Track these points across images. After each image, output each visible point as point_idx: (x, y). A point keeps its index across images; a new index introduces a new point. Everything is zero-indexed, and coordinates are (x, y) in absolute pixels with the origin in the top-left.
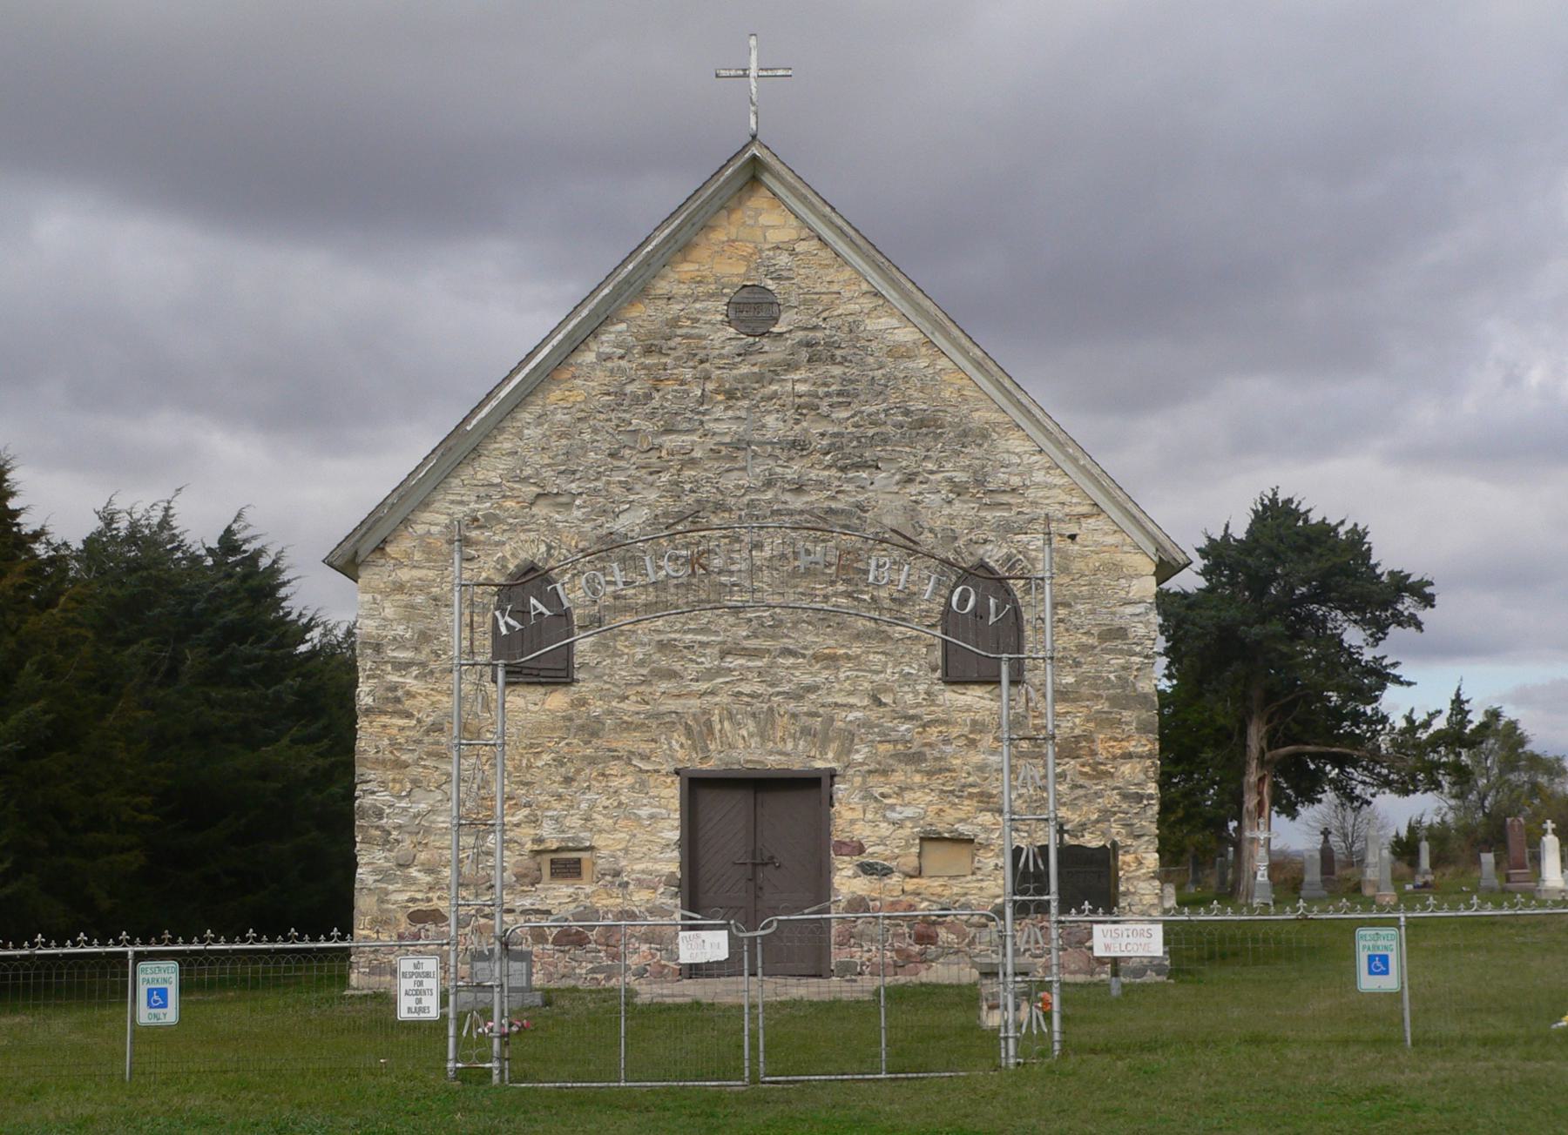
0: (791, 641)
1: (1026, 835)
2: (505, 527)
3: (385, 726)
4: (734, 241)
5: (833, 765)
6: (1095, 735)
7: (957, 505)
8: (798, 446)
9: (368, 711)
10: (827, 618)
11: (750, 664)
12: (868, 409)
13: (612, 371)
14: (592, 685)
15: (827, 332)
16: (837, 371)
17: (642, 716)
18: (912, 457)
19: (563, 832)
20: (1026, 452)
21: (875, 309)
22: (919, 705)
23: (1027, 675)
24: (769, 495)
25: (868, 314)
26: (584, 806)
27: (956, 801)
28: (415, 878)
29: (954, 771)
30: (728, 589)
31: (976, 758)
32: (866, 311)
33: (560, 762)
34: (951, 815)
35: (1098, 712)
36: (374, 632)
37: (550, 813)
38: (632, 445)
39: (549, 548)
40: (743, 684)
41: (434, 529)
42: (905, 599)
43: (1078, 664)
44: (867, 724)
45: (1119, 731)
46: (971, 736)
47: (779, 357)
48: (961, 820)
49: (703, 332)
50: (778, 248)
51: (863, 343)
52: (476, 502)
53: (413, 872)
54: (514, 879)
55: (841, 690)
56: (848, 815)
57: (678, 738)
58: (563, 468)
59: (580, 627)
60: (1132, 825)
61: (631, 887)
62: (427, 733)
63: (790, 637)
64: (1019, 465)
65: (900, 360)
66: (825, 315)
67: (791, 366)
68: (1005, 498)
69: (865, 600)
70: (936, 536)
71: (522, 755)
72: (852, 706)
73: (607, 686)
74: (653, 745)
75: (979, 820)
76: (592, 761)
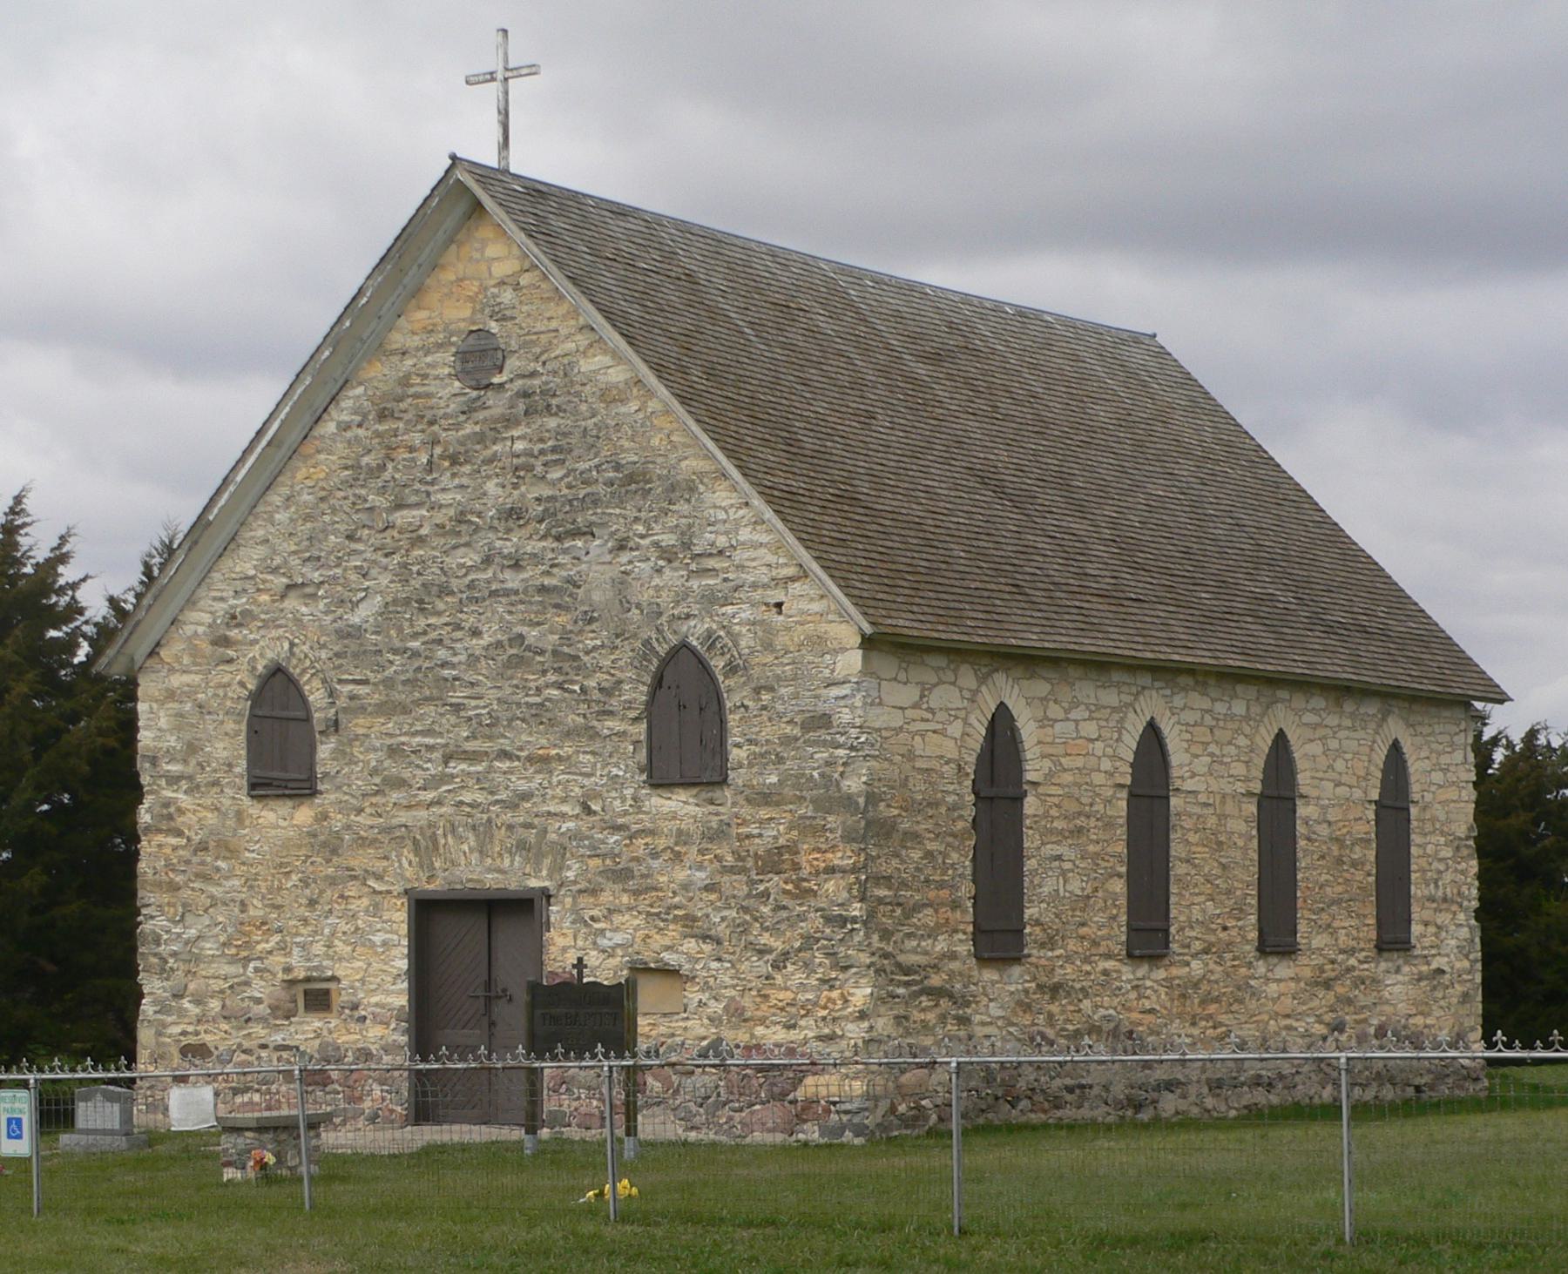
0: (507, 742)
1: (729, 965)
2: (260, 624)
3: (160, 846)
4: (462, 280)
5: (547, 884)
6: (800, 845)
7: (667, 572)
8: (513, 514)
9: (148, 829)
10: (540, 715)
11: (472, 769)
12: (582, 466)
13: (349, 442)
14: (332, 797)
15: (544, 378)
16: (552, 423)
17: (376, 831)
18: (622, 520)
19: (309, 960)
20: (732, 506)
21: (591, 345)
22: (626, 813)
23: (731, 774)
24: (490, 574)
25: (584, 353)
26: (327, 931)
27: (662, 924)
28: (186, 1010)
29: (661, 890)
30: (449, 685)
31: (681, 875)
32: (581, 349)
33: (305, 883)
34: (658, 941)
35: (802, 817)
36: (152, 744)
37: (298, 939)
38: (370, 524)
39: (292, 645)
40: (464, 792)
41: (201, 630)
42: (613, 689)
43: (780, 760)
44: (576, 836)
45: (822, 840)
46: (677, 848)
47: (497, 411)
48: (668, 948)
49: (432, 389)
50: (504, 283)
51: (578, 388)
52: (234, 598)
53: (185, 1003)
54: (269, 1011)
55: (553, 797)
56: (561, 942)
57: (408, 854)
58: (307, 555)
59: (321, 733)
60: (835, 954)
61: (368, 1021)
62: (195, 853)
63: (506, 737)
64: (725, 522)
65: (612, 405)
66: (543, 358)
67: (510, 421)
68: (711, 563)
69: (575, 691)
70: (642, 611)
71: (273, 875)
72: (563, 816)
73: (347, 797)
74: (385, 863)
75: (684, 948)
76: (332, 881)
